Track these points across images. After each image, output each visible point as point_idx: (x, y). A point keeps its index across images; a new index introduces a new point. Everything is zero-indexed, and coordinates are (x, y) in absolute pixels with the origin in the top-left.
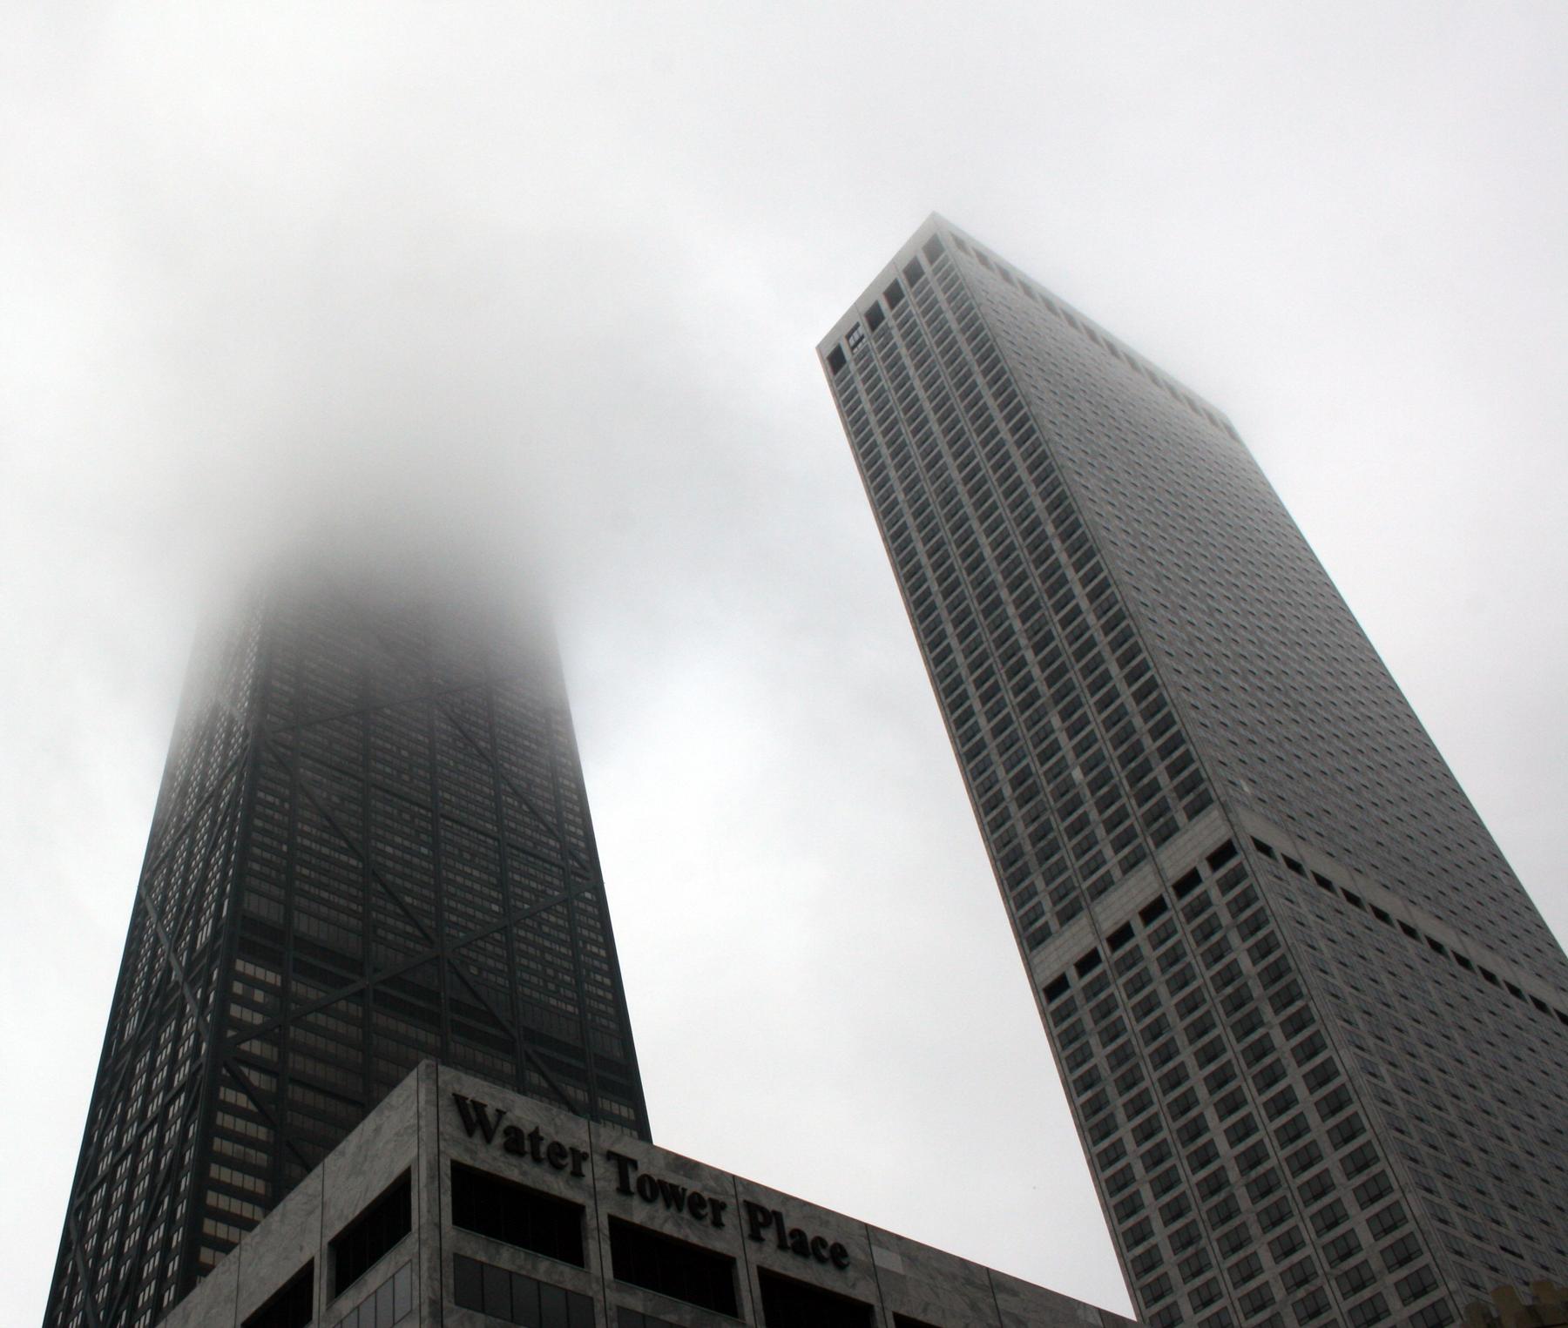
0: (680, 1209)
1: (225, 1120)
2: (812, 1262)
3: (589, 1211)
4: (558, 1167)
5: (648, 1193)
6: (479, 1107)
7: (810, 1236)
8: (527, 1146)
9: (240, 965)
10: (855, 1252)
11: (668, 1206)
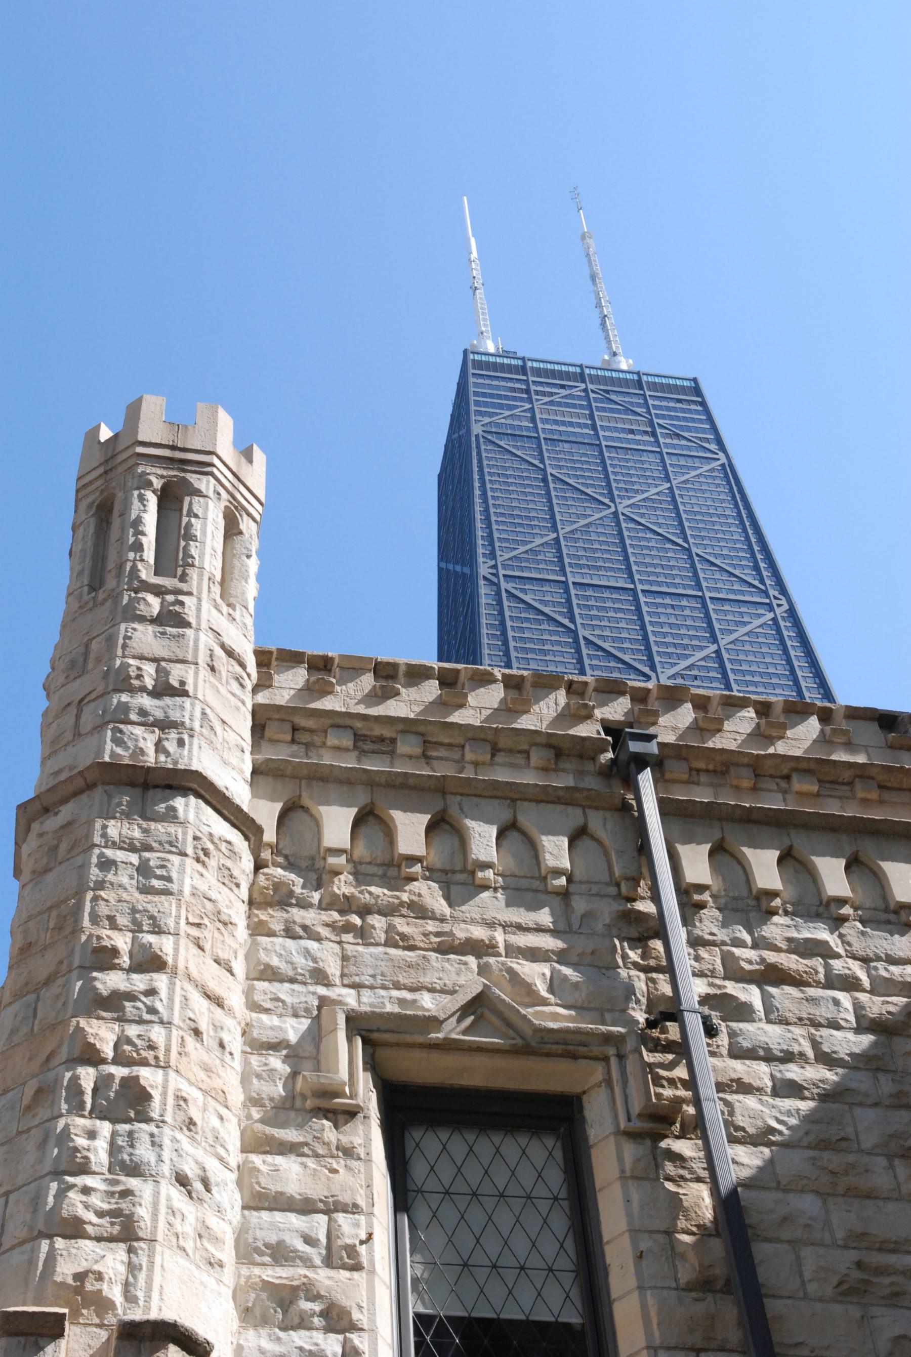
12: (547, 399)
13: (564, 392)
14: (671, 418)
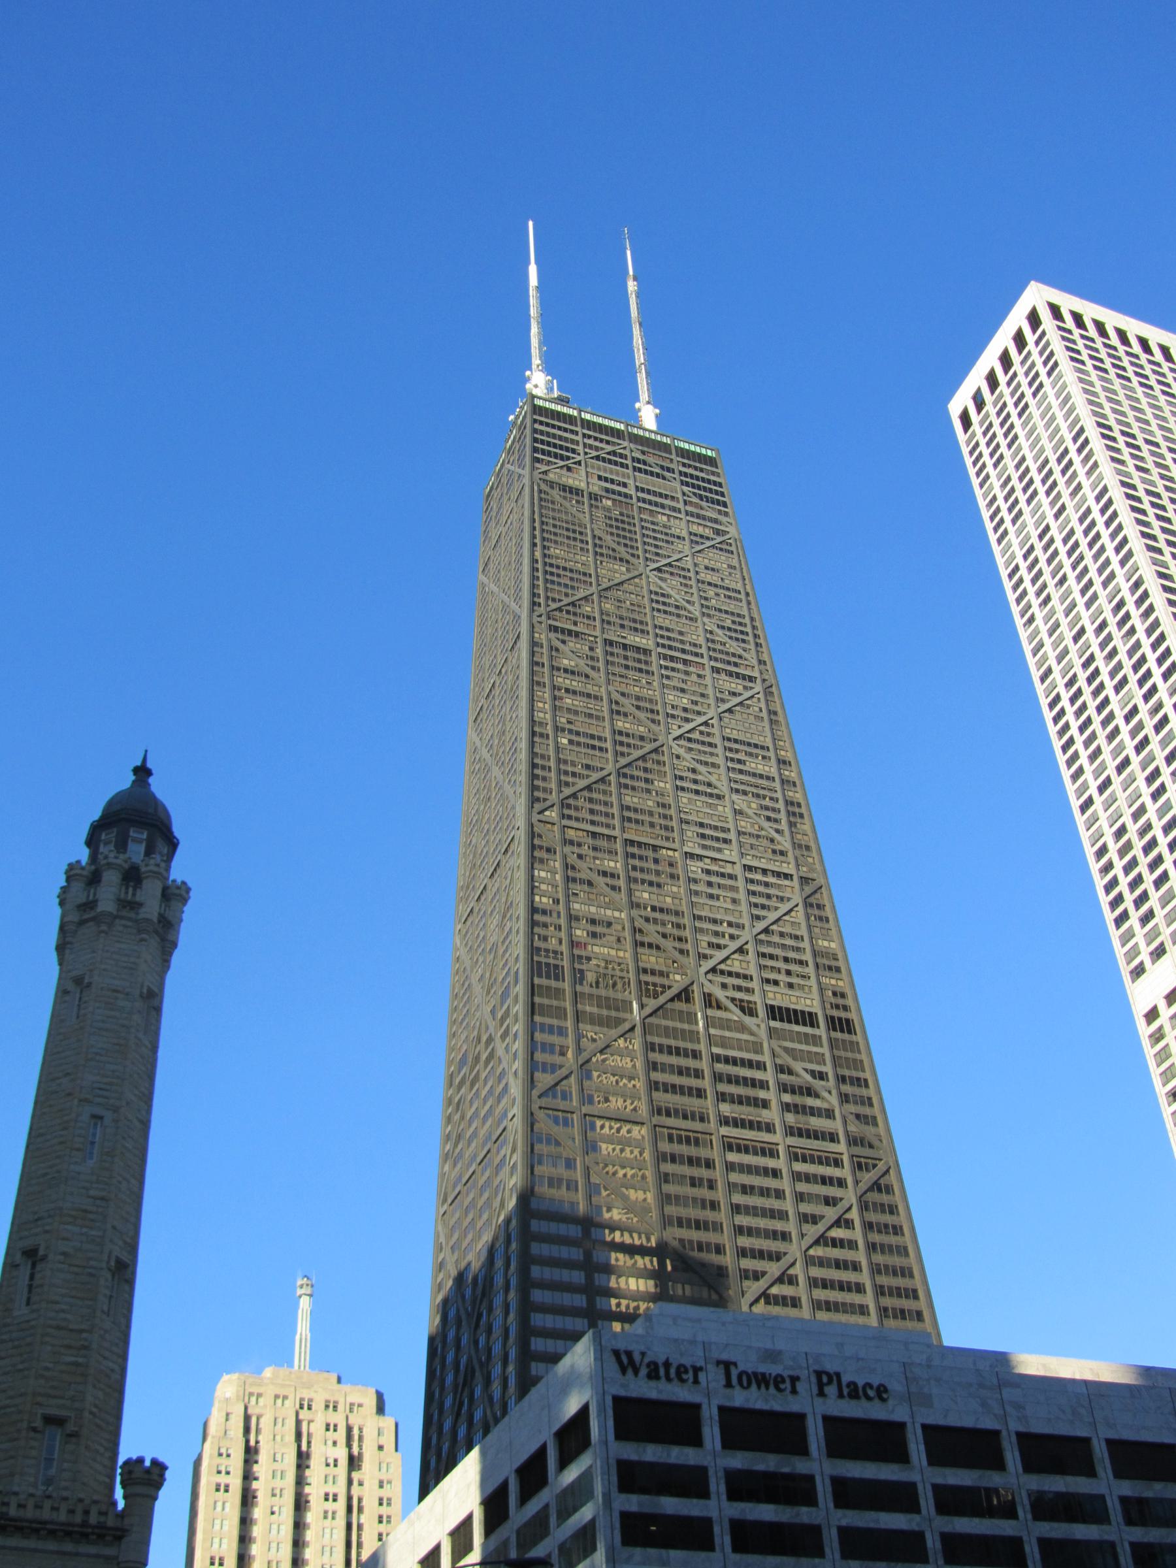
0: (767, 1388)
2: (863, 1402)
3: (705, 1407)
4: (682, 1381)
5: (745, 1384)
6: (629, 1354)
7: (860, 1384)
8: (662, 1372)
10: (896, 1386)
11: (759, 1387)
12: (594, 453)
13: (609, 448)
14: (693, 486)
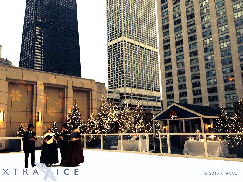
1: (36, 45)
9: (37, 27)
